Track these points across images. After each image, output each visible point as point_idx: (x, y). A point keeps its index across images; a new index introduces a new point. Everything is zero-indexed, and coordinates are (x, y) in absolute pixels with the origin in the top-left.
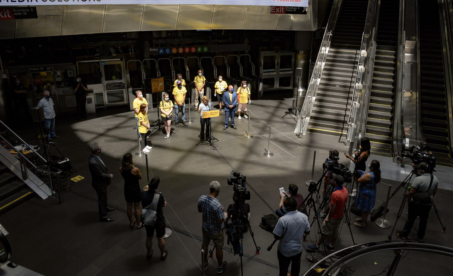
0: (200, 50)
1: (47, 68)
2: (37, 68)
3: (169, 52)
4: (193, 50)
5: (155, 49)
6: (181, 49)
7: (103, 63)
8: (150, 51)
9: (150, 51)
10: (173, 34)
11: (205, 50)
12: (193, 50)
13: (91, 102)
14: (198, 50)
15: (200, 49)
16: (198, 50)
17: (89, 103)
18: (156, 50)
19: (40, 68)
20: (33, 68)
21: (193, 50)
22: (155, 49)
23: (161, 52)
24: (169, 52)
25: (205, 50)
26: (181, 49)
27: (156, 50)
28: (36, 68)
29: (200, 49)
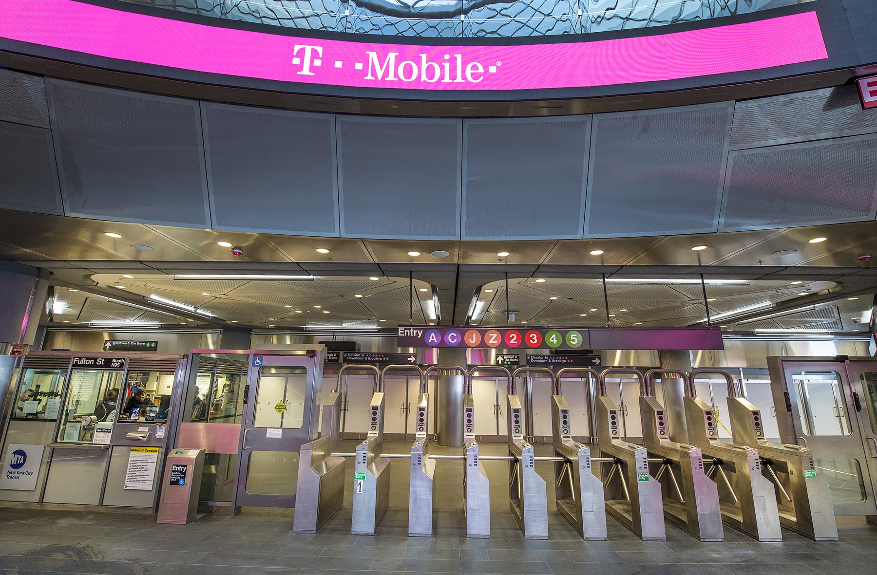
0: (555, 341)
1: (114, 360)
2: (90, 359)
3: (455, 340)
4: (534, 341)
5: (415, 331)
6: (495, 335)
7: (258, 361)
8: (399, 335)
9: (399, 335)
10: (508, 360)
11: (574, 341)
12: (531, 338)
13: (181, 482)
14: (551, 340)
15: (554, 336)
16: (551, 340)
17: (175, 483)
18: (417, 333)
19: (96, 359)
20: (81, 358)
21: (534, 341)
22: (415, 331)
23: (431, 339)
24: (455, 340)
25: (574, 341)
26: (495, 335)
27: (417, 333)
28: (87, 359)
29: (554, 336)
